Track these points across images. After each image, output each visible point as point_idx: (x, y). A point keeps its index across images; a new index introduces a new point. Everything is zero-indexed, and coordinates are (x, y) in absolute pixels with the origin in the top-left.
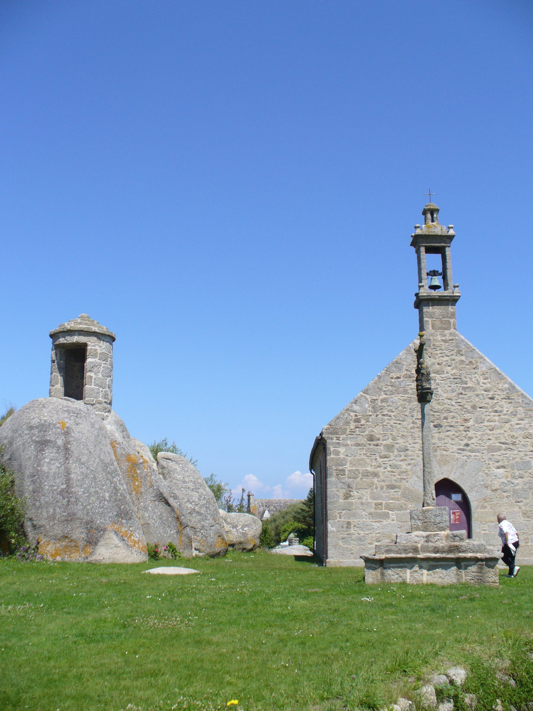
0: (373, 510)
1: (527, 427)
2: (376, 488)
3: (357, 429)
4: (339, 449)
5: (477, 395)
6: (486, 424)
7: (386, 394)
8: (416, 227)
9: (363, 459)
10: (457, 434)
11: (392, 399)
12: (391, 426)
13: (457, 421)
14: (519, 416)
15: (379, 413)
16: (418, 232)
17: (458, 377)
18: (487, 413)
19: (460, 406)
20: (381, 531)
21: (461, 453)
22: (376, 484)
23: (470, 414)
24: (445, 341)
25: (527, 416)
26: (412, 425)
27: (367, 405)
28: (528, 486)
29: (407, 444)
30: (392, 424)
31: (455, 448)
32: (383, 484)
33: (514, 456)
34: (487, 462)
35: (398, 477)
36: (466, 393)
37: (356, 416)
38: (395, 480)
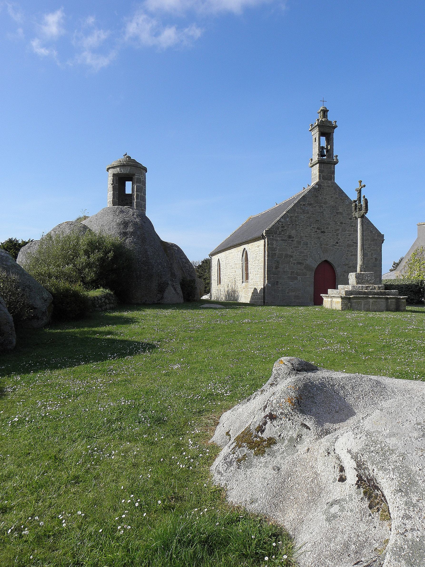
29: (308, 241)
37: (282, 224)
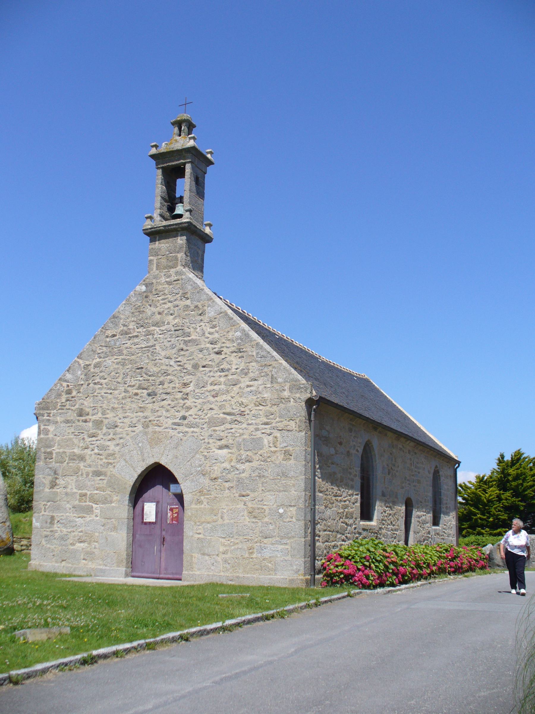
0: (77, 502)
1: (260, 389)
2: (82, 475)
3: (68, 402)
4: (49, 427)
5: (201, 351)
6: (209, 388)
7: (100, 357)
8: (153, 146)
9: (70, 439)
10: (173, 404)
11: (105, 363)
12: (102, 396)
13: (174, 386)
14: (251, 375)
15: (90, 381)
16: (154, 151)
17: (180, 328)
18: (211, 374)
19: (180, 365)
20: (83, 529)
21: (176, 429)
22: (82, 469)
23: (191, 376)
24: (169, 283)
25: (263, 374)
26: (123, 394)
27: (80, 372)
28: (257, 474)
29: (116, 419)
30: (103, 394)
31: (170, 421)
32: (90, 470)
33: (241, 431)
34: (206, 440)
35: (104, 460)
36: (188, 348)
38: (101, 465)
